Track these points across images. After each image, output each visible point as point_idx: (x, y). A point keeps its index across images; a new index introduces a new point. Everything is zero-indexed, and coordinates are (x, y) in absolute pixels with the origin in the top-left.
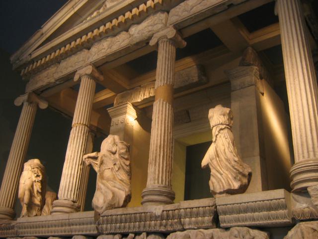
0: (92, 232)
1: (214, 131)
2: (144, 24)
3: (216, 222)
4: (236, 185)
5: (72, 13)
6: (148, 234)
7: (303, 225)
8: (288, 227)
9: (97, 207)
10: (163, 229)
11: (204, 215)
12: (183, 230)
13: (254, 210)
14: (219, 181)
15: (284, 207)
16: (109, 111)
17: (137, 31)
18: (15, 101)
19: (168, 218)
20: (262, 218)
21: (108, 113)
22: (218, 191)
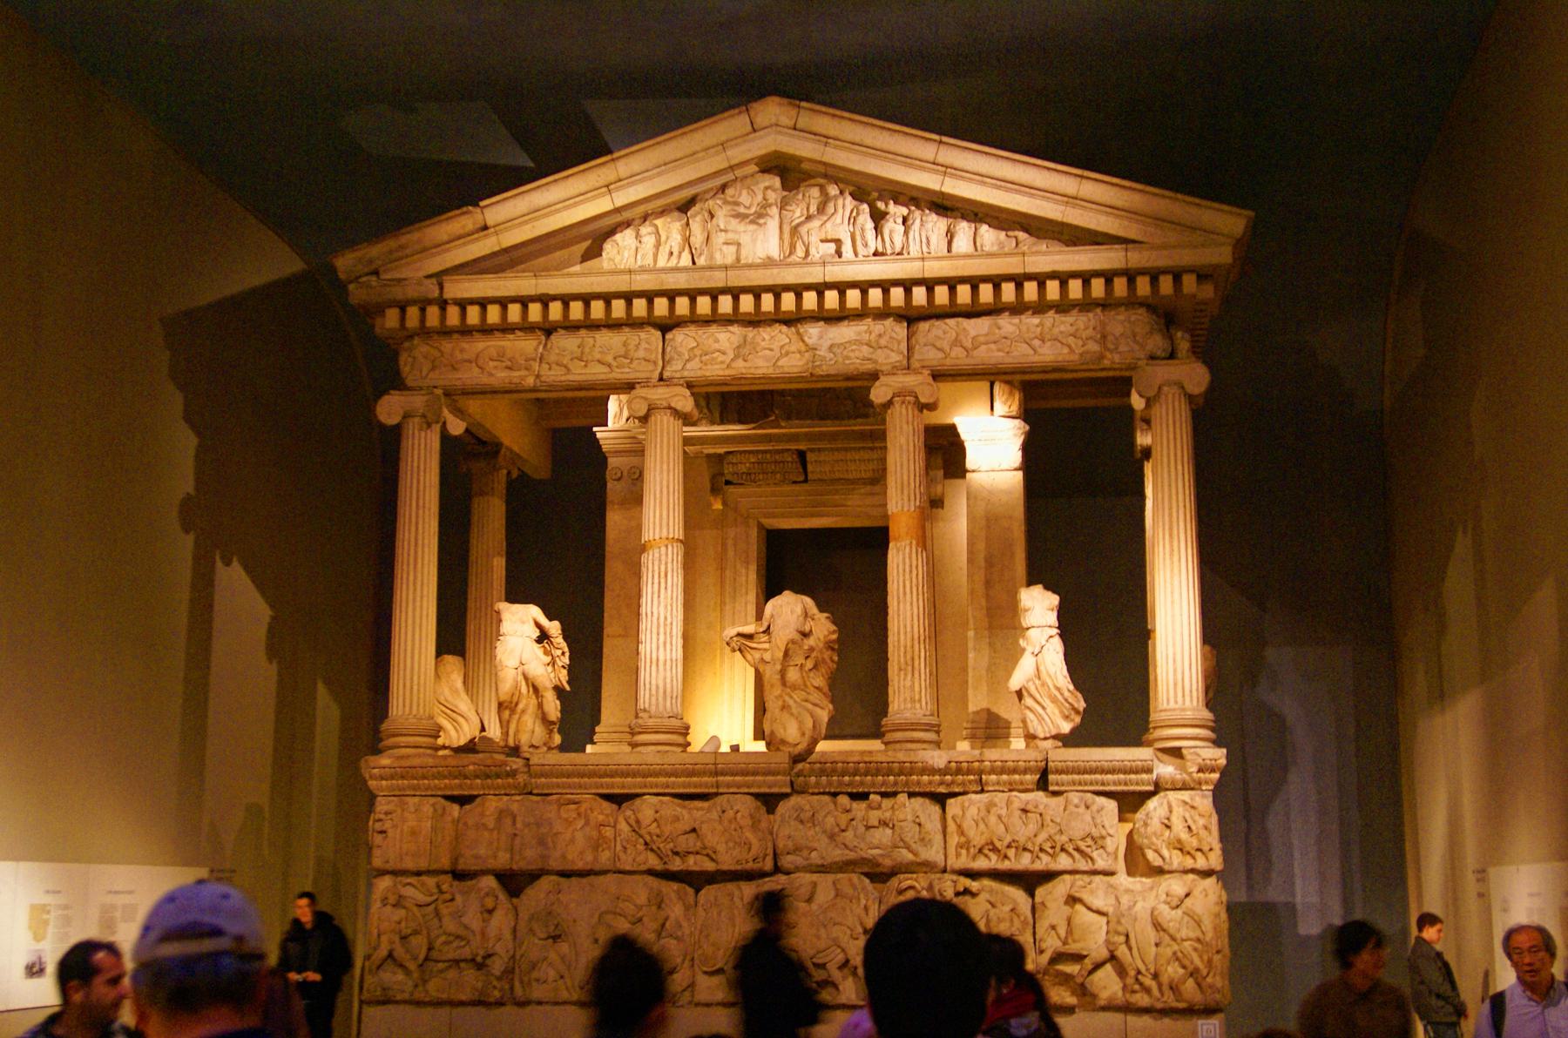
0: (775, 790)
1: (1031, 633)
2: (845, 332)
3: (1043, 784)
4: (1066, 728)
5: (603, 205)
6: (911, 795)
7: (1171, 794)
8: (1146, 796)
9: (783, 742)
10: (942, 790)
11: (1025, 771)
12: (982, 791)
13: (1103, 771)
14: (1040, 719)
15: (1149, 771)
16: (599, 435)
17: (826, 344)
18: (379, 409)
19: (959, 771)
20: (1113, 782)
21: (597, 441)
22: (1042, 735)
